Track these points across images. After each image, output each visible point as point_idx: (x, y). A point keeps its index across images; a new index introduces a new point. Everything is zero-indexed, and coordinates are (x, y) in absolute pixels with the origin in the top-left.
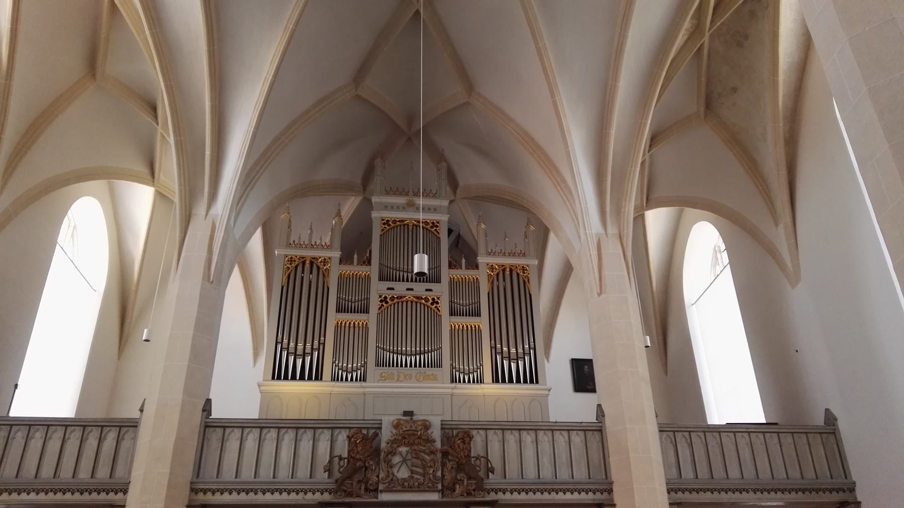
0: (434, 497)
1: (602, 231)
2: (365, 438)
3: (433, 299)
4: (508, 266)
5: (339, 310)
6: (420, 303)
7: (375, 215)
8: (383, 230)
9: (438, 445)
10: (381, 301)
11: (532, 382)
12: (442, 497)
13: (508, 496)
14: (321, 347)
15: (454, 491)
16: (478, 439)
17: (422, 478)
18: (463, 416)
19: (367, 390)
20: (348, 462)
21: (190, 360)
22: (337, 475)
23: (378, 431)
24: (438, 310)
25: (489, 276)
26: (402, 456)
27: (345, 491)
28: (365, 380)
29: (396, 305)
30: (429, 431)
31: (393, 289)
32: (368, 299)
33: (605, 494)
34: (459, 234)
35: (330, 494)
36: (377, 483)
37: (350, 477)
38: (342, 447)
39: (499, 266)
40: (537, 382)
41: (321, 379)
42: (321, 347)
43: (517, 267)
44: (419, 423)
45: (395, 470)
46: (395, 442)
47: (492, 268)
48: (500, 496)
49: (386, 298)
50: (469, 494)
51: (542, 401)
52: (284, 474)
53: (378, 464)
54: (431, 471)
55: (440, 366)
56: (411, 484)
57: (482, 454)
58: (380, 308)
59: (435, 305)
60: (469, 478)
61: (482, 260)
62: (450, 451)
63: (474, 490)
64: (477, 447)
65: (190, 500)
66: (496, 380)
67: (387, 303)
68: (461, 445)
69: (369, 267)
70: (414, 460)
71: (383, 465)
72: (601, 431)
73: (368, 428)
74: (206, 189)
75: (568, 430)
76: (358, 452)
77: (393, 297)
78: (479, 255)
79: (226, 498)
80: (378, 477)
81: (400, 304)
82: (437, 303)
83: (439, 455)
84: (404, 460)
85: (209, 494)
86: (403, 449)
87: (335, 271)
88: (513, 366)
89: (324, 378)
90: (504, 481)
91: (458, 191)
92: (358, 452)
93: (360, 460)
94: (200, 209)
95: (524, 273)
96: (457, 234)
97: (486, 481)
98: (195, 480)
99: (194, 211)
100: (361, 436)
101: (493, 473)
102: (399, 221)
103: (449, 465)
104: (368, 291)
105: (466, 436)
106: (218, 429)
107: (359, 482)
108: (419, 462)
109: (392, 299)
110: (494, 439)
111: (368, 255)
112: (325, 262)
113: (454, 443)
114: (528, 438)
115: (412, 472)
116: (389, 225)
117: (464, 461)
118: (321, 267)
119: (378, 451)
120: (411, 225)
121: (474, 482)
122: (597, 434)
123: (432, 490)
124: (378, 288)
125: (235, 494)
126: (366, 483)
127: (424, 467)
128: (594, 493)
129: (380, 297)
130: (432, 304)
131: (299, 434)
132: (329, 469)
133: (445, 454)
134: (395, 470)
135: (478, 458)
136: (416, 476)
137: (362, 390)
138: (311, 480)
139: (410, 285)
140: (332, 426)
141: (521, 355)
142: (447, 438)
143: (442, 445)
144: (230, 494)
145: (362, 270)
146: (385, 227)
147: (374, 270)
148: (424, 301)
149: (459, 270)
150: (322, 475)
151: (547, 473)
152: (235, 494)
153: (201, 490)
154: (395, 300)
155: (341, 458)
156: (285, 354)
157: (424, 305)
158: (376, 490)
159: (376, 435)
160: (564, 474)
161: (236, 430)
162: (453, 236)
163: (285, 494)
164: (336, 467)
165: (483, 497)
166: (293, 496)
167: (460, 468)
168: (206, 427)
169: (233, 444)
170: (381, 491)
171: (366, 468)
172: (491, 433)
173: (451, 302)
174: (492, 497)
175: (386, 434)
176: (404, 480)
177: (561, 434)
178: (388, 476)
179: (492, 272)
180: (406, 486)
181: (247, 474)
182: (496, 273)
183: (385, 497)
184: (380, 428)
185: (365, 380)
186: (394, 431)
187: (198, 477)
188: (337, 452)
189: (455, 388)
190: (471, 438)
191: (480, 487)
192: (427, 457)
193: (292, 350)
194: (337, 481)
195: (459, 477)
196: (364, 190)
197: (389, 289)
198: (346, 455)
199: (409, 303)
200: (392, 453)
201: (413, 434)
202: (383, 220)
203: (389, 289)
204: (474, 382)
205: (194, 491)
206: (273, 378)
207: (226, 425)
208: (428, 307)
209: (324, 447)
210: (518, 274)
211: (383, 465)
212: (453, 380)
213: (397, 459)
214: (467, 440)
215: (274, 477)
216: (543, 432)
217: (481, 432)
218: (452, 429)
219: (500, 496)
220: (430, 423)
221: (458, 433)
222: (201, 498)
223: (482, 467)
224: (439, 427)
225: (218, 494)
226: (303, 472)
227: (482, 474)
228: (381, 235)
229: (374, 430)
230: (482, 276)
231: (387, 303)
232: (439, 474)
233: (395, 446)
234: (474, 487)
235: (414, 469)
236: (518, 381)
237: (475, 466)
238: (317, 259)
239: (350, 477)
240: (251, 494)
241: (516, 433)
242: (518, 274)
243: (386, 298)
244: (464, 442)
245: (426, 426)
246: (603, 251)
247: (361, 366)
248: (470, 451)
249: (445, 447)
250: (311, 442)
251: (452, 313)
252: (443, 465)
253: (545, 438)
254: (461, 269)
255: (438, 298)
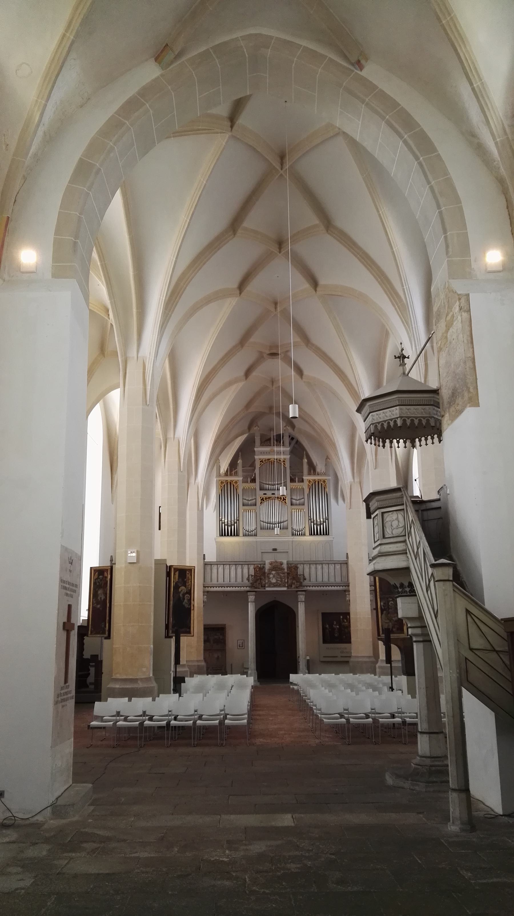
0: (285, 589)
1: (352, 480)
2: (260, 568)
3: (284, 498)
4: (317, 480)
5: (243, 505)
6: (278, 500)
7: (256, 457)
8: (260, 465)
9: (286, 570)
10: (261, 500)
11: (326, 534)
12: (288, 589)
13: (311, 588)
14: (238, 522)
15: (292, 586)
16: (300, 567)
17: (280, 582)
18: (295, 557)
19: (257, 540)
20: (255, 577)
21: (197, 542)
22: (251, 581)
23: (264, 565)
24: (286, 503)
25: (309, 485)
26: (273, 574)
27: (254, 587)
28: (256, 535)
29: (268, 501)
30: (283, 566)
31: (265, 494)
32: (255, 499)
33: (347, 587)
34: (297, 440)
35: (249, 587)
36: (265, 584)
37: (256, 582)
38: (252, 572)
39: (313, 480)
40: (329, 534)
41: (239, 535)
42: (238, 522)
43: (321, 481)
44: (279, 563)
45: (271, 580)
46: (271, 570)
47: (310, 481)
48: (308, 588)
49: (263, 498)
50: (297, 587)
51: (330, 543)
52: (233, 580)
53: (265, 578)
54: (284, 580)
55: (287, 529)
56: (277, 584)
57: (302, 573)
58: (261, 503)
59: (284, 501)
60: (297, 582)
61: (306, 478)
62: (290, 573)
63: (299, 586)
64: (300, 572)
65: (203, 590)
66: (311, 534)
67: (264, 500)
68: (294, 571)
69: (255, 484)
70: (277, 576)
71: (267, 578)
72: (347, 564)
73: (260, 564)
74: (194, 473)
75: (334, 564)
76: (258, 574)
77: (266, 498)
78: (304, 476)
79: (215, 589)
80: (265, 582)
81: (269, 501)
82: (285, 500)
83: (286, 574)
84: (274, 576)
85: (209, 588)
86: (274, 572)
87: (241, 486)
88: (318, 527)
89: (240, 535)
90: (309, 583)
91: (295, 429)
92: (258, 574)
93: (259, 576)
94: (192, 480)
95: (324, 483)
96: (296, 440)
97: (303, 583)
98: (204, 583)
99: (190, 482)
100: (258, 568)
101: (306, 580)
102: (267, 460)
103: (290, 578)
104: (256, 495)
105: (296, 568)
106: (209, 565)
107: (259, 584)
108: (279, 577)
109: (266, 499)
110: (307, 567)
111: (254, 475)
112: (236, 482)
113: (292, 570)
114: (319, 567)
115: (277, 580)
116: (263, 462)
117: (295, 576)
118: (235, 485)
119: (265, 573)
120: (272, 462)
121: (299, 583)
122: (345, 565)
123: (284, 586)
124: (260, 494)
125: (218, 588)
126: (261, 584)
127: (281, 578)
128: (343, 587)
129: (261, 498)
130: (283, 500)
131: (237, 567)
132: (248, 579)
133: (288, 574)
134: (271, 580)
135: (300, 575)
136: (279, 582)
137: (255, 540)
138: (242, 583)
139: (273, 492)
140: (248, 564)
141: (322, 522)
142: (289, 568)
143: (287, 571)
144: (216, 588)
145: (252, 485)
146: (261, 464)
147: (257, 485)
148: (279, 499)
149: (295, 483)
150: (246, 581)
151: (326, 579)
152: (218, 588)
153: (207, 586)
154: (267, 499)
155: (252, 576)
156: (223, 525)
157: (280, 501)
158: (265, 586)
159: (264, 567)
160: (332, 580)
161: (215, 565)
162: (294, 441)
163: (234, 588)
164: (251, 579)
165: (302, 589)
166: (237, 588)
167: (294, 578)
168: (205, 564)
169: (215, 571)
170: (267, 587)
171: (261, 579)
172: (305, 565)
173: (291, 499)
174: (305, 588)
175: (267, 567)
176: (274, 583)
177: (331, 565)
178: (268, 582)
179: (310, 483)
180: (275, 585)
181: (221, 581)
182: (311, 484)
183: (268, 589)
184: (265, 564)
185: (256, 535)
186: (270, 566)
187: (205, 582)
188: (250, 574)
189: (293, 538)
190: (297, 568)
191: (301, 585)
192: (282, 575)
193: (226, 523)
194: (251, 583)
195: (293, 582)
196: (249, 431)
197: (264, 494)
198: (253, 574)
199: (273, 500)
200: (270, 574)
201: (277, 567)
202: (260, 460)
203: (264, 494)
204: (301, 535)
205: (204, 587)
206: (220, 536)
207: (211, 564)
208: (281, 502)
209: (246, 571)
210: (322, 484)
211: (267, 578)
212: (293, 535)
213: (271, 576)
214: (296, 569)
215: (230, 582)
216: (324, 565)
217: (302, 565)
218: (291, 564)
219: (308, 588)
220: (283, 563)
221: (293, 566)
222: (207, 589)
223: (302, 578)
224: (286, 563)
225: (212, 588)
226: (239, 580)
227: (302, 581)
228: (259, 467)
229: (262, 565)
230: (305, 485)
231: (264, 500)
232: (286, 581)
233: (270, 571)
234: (298, 585)
235: (278, 579)
236: (321, 534)
237: (299, 578)
238: (233, 481)
239: (256, 582)
240: (223, 588)
241: (315, 565)
242: (322, 484)
243: (263, 498)
244: (295, 570)
245: (281, 564)
246: (352, 490)
247: (255, 529)
248: (297, 573)
249: (288, 572)
250: (241, 569)
251: (292, 504)
252: (288, 578)
253: (325, 567)
254: (296, 482)
255: (286, 497)
